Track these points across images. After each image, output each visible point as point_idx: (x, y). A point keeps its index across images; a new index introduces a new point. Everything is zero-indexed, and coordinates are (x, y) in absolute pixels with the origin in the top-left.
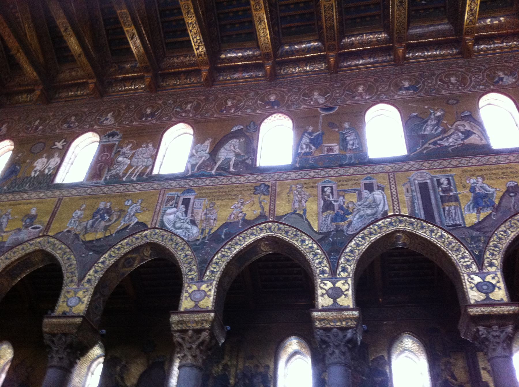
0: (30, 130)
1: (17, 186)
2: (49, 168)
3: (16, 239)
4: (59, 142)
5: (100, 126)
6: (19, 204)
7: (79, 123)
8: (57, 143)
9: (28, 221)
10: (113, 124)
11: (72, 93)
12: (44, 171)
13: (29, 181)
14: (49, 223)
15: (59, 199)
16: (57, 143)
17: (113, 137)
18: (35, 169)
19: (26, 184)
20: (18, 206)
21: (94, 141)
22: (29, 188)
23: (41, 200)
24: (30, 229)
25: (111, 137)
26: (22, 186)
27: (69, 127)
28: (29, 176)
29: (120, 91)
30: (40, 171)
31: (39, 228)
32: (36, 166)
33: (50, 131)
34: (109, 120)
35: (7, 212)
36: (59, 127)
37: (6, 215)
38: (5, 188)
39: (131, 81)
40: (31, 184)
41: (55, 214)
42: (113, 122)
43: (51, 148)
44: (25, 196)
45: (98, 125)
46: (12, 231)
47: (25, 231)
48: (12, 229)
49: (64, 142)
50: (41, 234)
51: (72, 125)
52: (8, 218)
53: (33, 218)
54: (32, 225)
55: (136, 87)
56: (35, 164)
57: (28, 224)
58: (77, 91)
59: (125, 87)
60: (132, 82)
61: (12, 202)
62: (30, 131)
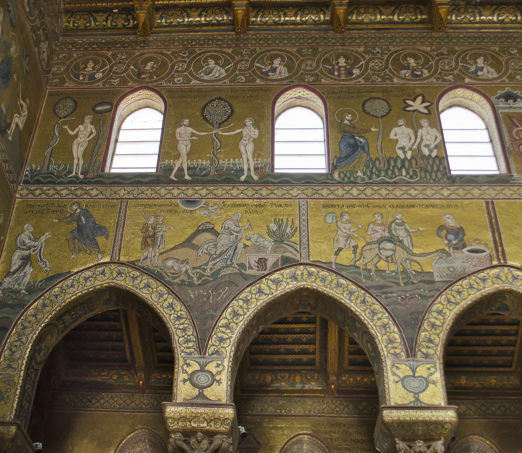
0: (336, 73)
1: (383, 173)
2: (427, 146)
3: (452, 269)
4: (414, 100)
5: (475, 79)
6: (413, 206)
7: (429, 70)
8: (410, 102)
9: (451, 237)
10: (498, 78)
11: (383, 17)
12: (419, 149)
13: (403, 166)
14: (498, 244)
15: (487, 203)
16: (410, 102)
17: (515, 101)
18: (399, 145)
19: (400, 170)
20: (412, 210)
21: (453, 103)
22: (411, 177)
23: (452, 202)
24: (465, 250)
25: (511, 101)
26: (393, 172)
27: (413, 75)
28: (395, 156)
29: (471, 22)
30: (410, 149)
31: (484, 251)
32: (397, 141)
33: (380, 80)
34: (485, 70)
35: (396, 219)
36: (395, 75)
37: (397, 224)
38: (360, 174)
39: (494, 7)
40: (411, 173)
41: (498, 229)
42: (495, 75)
43: (404, 109)
44: (413, 192)
45: (471, 78)
46: (429, 254)
47: (458, 254)
48: (427, 251)
49: (423, 102)
50: (495, 263)
51: (419, 73)
52: (407, 231)
53: (459, 232)
54: (464, 246)
55: (500, 18)
56: (392, 136)
57: (454, 242)
58: (393, 14)
59: (481, 15)
60: (496, 9)
61: (395, 202)
62: (339, 76)
